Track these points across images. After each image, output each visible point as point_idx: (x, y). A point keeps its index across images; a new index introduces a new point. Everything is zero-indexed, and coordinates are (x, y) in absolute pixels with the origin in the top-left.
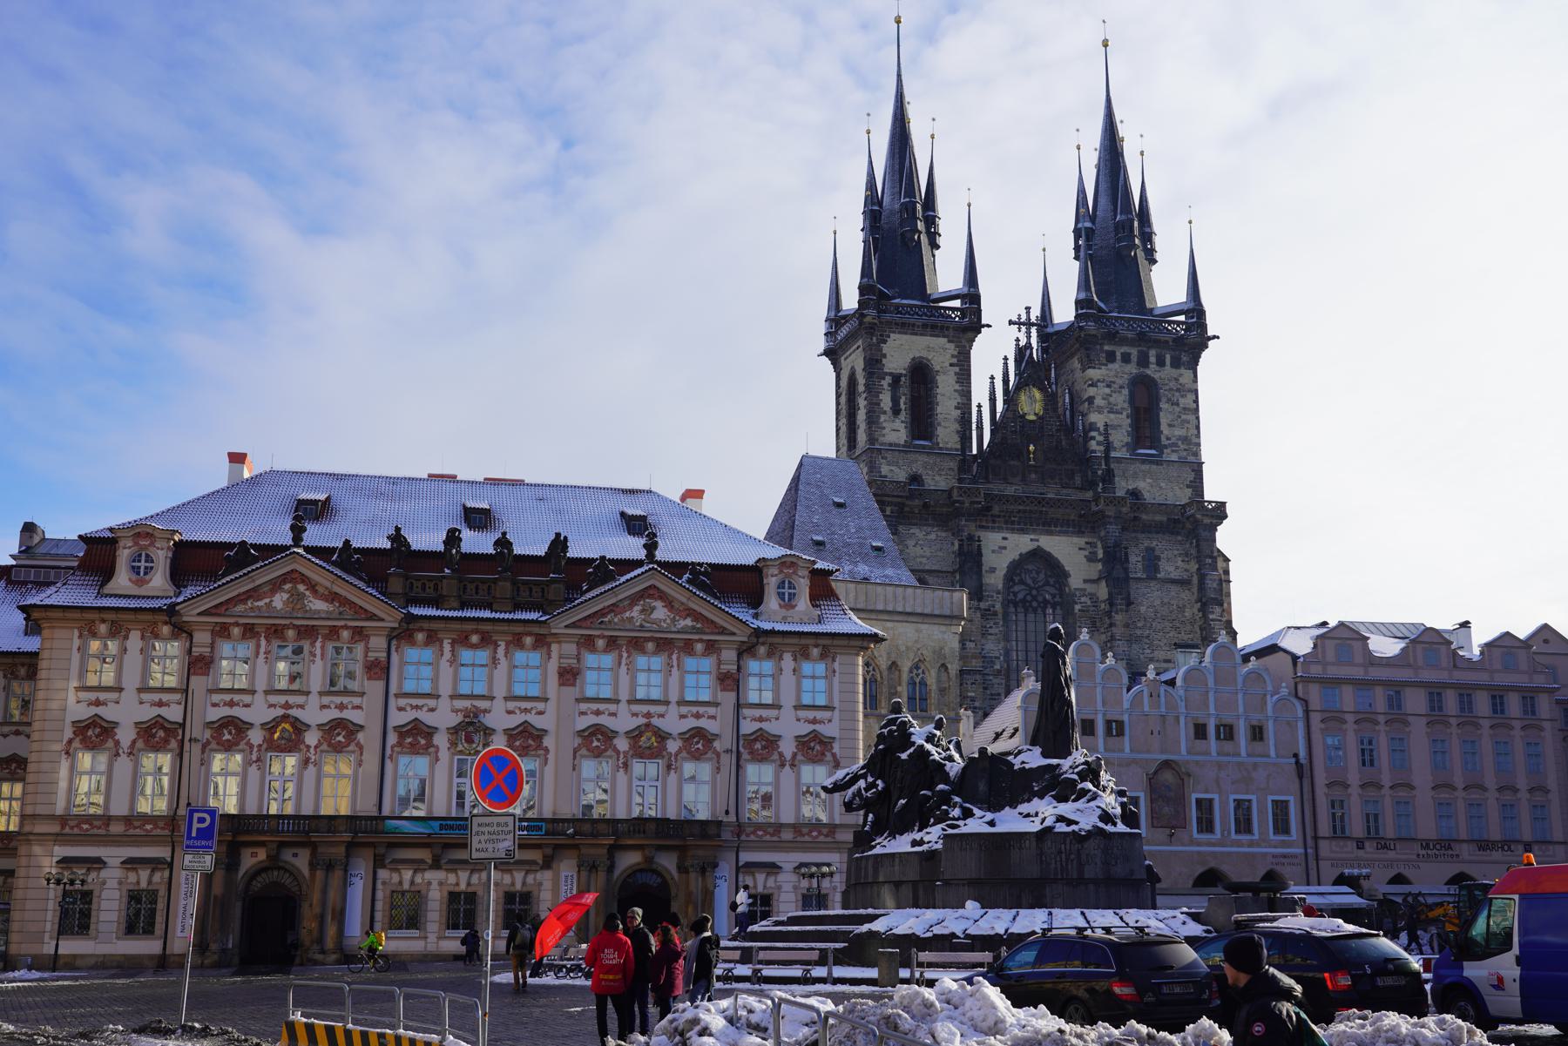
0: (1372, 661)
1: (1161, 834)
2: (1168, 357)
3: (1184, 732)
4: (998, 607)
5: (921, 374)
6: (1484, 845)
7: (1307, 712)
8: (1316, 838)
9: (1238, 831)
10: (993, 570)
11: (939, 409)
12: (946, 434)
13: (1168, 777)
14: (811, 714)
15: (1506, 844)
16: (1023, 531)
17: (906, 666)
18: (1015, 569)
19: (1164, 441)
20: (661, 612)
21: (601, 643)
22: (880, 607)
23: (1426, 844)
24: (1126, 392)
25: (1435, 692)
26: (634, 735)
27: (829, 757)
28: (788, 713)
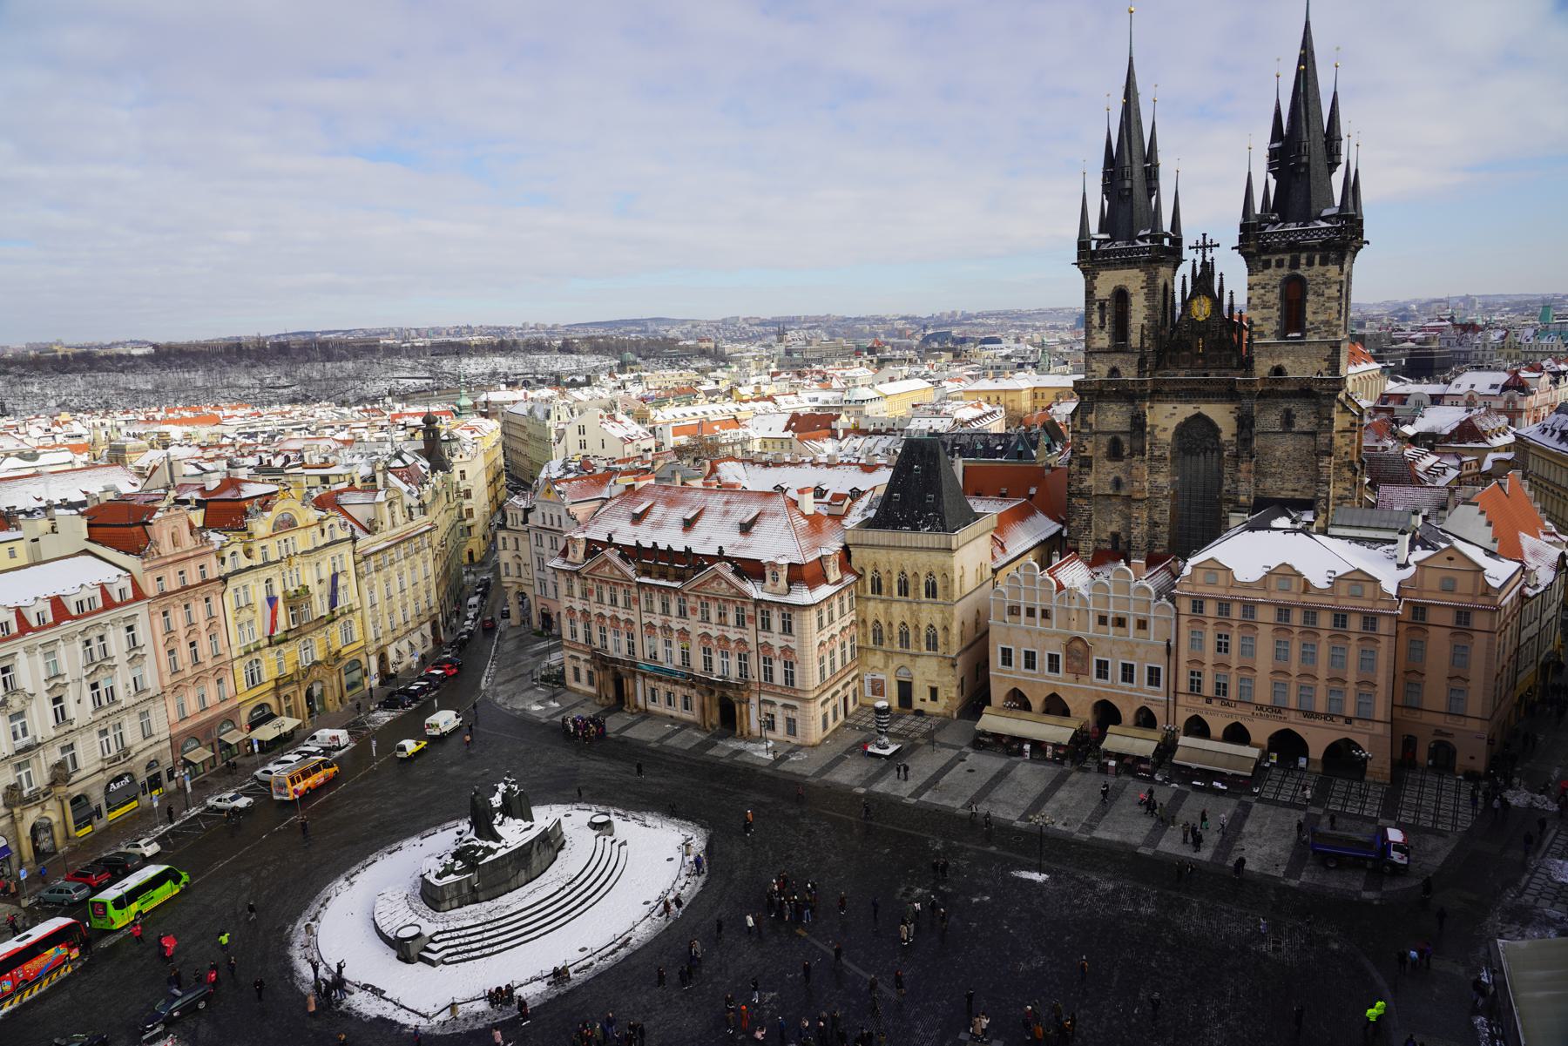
0: (1233, 583)
1: (1072, 677)
2: (1317, 258)
3: (1092, 621)
4: (1168, 454)
5: (1121, 296)
6: (1310, 714)
7: (1178, 615)
8: (1176, 692)
9: (1124, 679)
10: (1165, 430)
11: (1132, 321)
12: (1135, 339)
13: (1078, 645)
15: (1328, 716)
16: (1188, 402)
18: (1183, 430)
19: (1308, 326)
20: (724, 585)
23: (1261, 707)
24: (1278, 290)
25: (1284, 611)
28: (776, 636)
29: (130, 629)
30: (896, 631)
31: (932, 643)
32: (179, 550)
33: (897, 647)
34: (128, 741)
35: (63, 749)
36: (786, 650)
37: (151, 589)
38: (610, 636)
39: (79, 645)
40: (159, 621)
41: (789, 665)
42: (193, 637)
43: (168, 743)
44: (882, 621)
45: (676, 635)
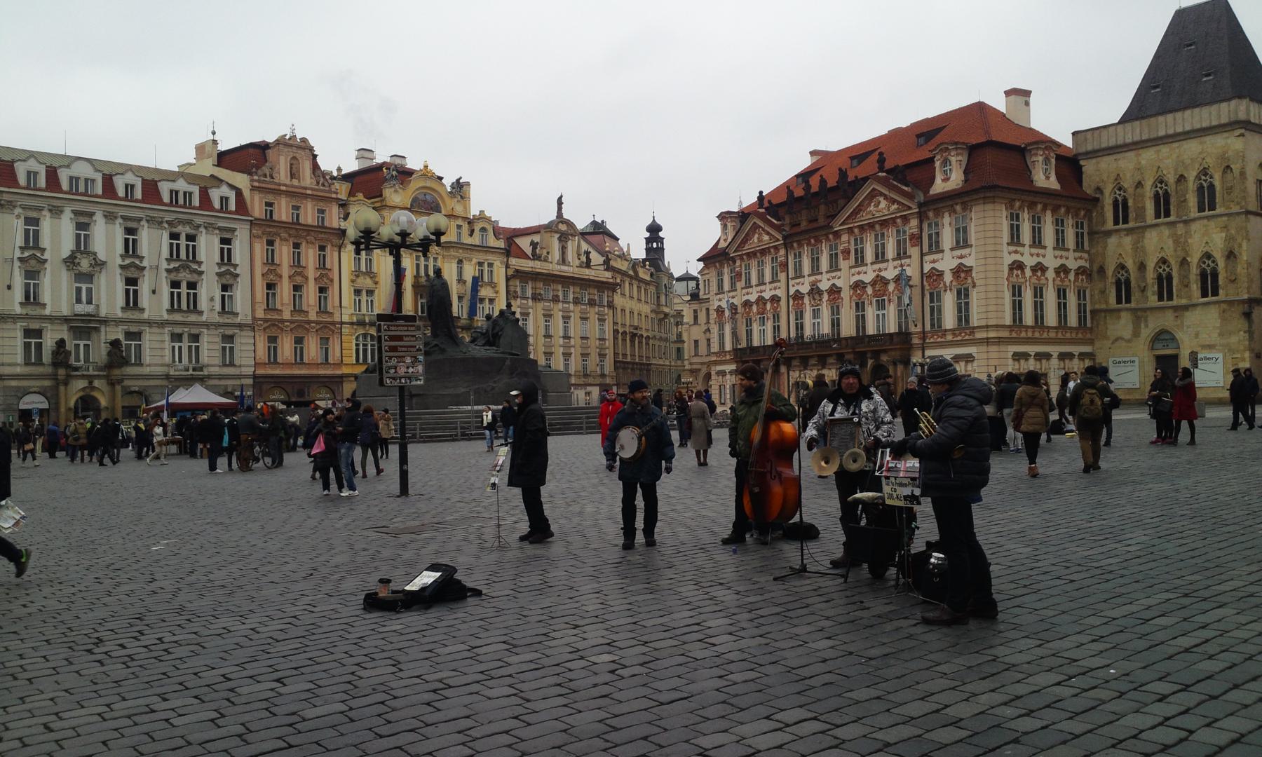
14: (958, 253)
17: (1191, 176)
20: (883, 204)
21: (856, 230)
22: (1162, 133)
26: (873, 283)
27: (969, 281)
29: (226, 241)
30: (1151, 275)
31: (1209, 282)
32: (295, 182)
33: (1153, 300)
34: (205, 357)
35: (130, 335)
36: (961, 272)
37: (257, 210)
38: (756, 328)
39: (166, 235)
40: (260, 248)
41: (963, 295)
42: (299, 279)
43: (250, 381)
44: (1130, 264)
45: (825, 297)
